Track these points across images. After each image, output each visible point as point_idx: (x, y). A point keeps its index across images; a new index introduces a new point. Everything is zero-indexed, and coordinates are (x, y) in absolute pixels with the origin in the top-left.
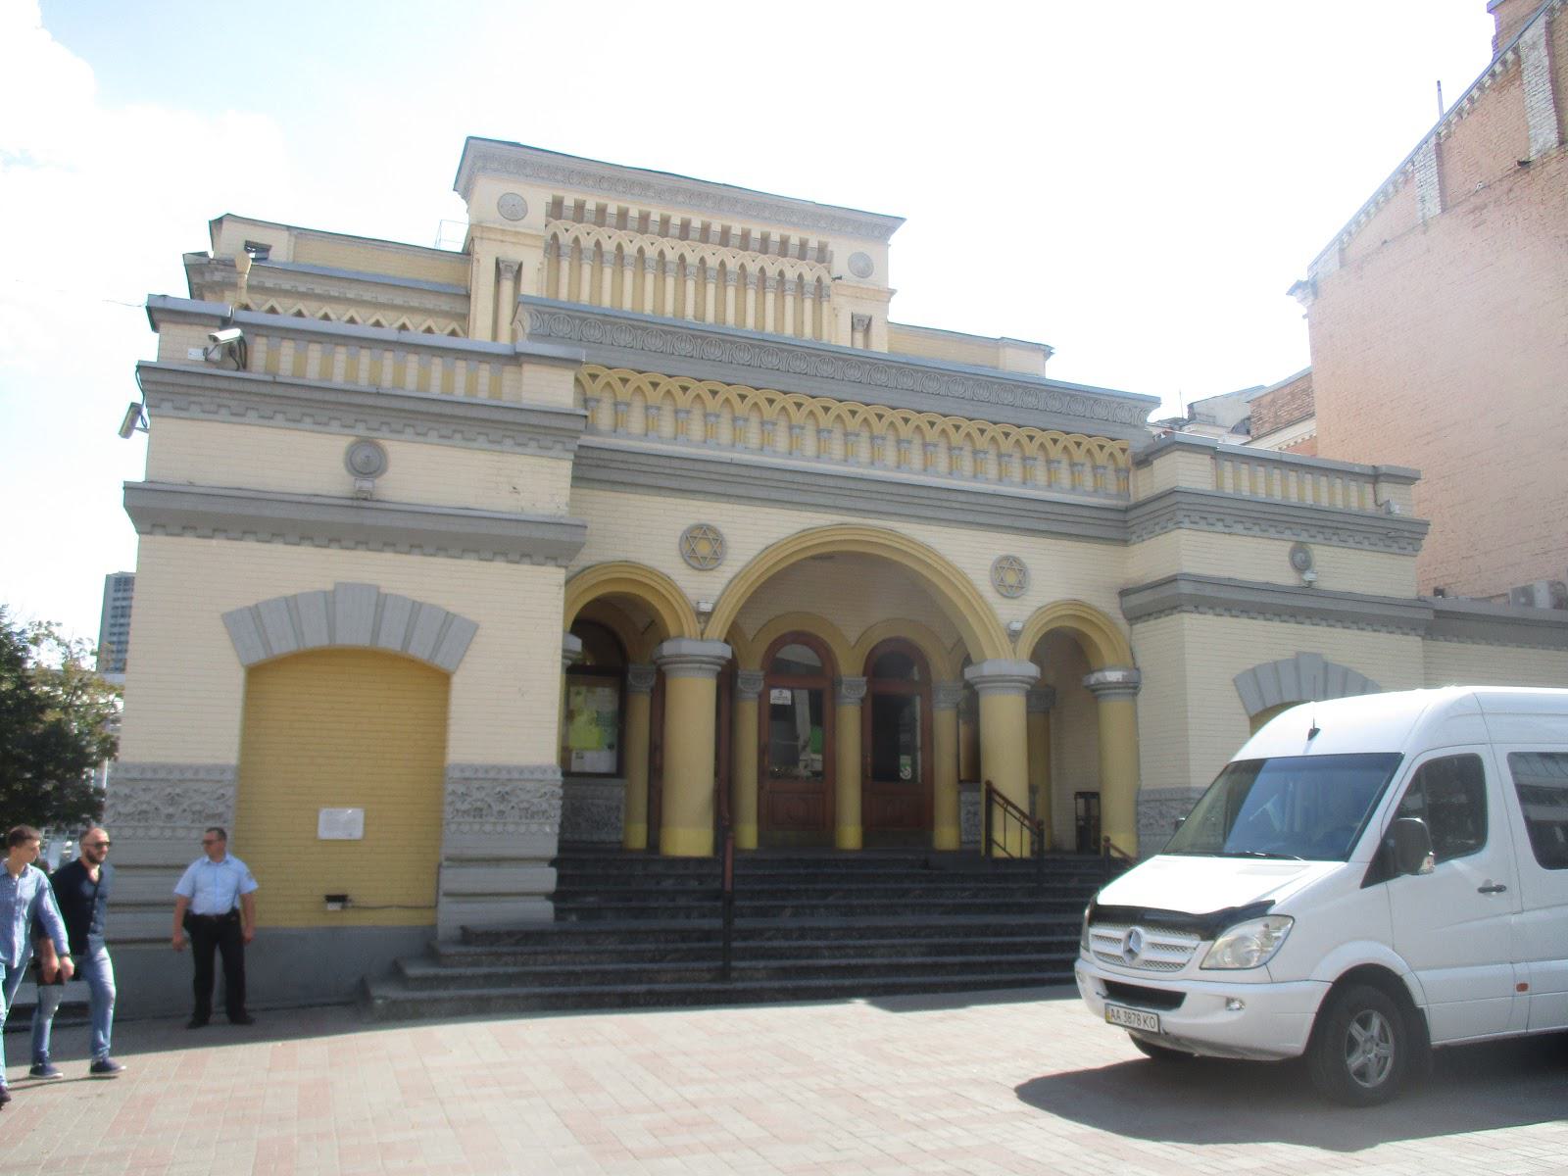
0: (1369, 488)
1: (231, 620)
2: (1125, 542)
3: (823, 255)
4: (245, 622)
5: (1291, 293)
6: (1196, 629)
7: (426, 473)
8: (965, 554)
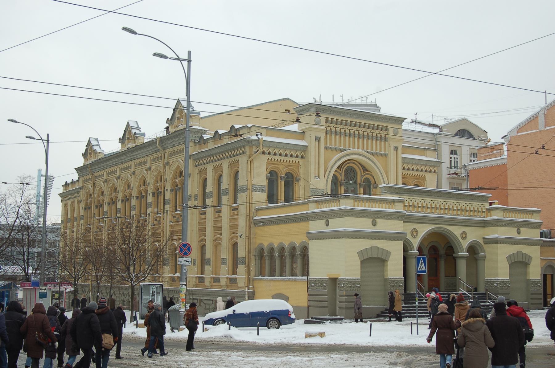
3: (387, 129)
4: (360, 253)
5: (502, 138)
7: (384, 226)
8: (456, 231)
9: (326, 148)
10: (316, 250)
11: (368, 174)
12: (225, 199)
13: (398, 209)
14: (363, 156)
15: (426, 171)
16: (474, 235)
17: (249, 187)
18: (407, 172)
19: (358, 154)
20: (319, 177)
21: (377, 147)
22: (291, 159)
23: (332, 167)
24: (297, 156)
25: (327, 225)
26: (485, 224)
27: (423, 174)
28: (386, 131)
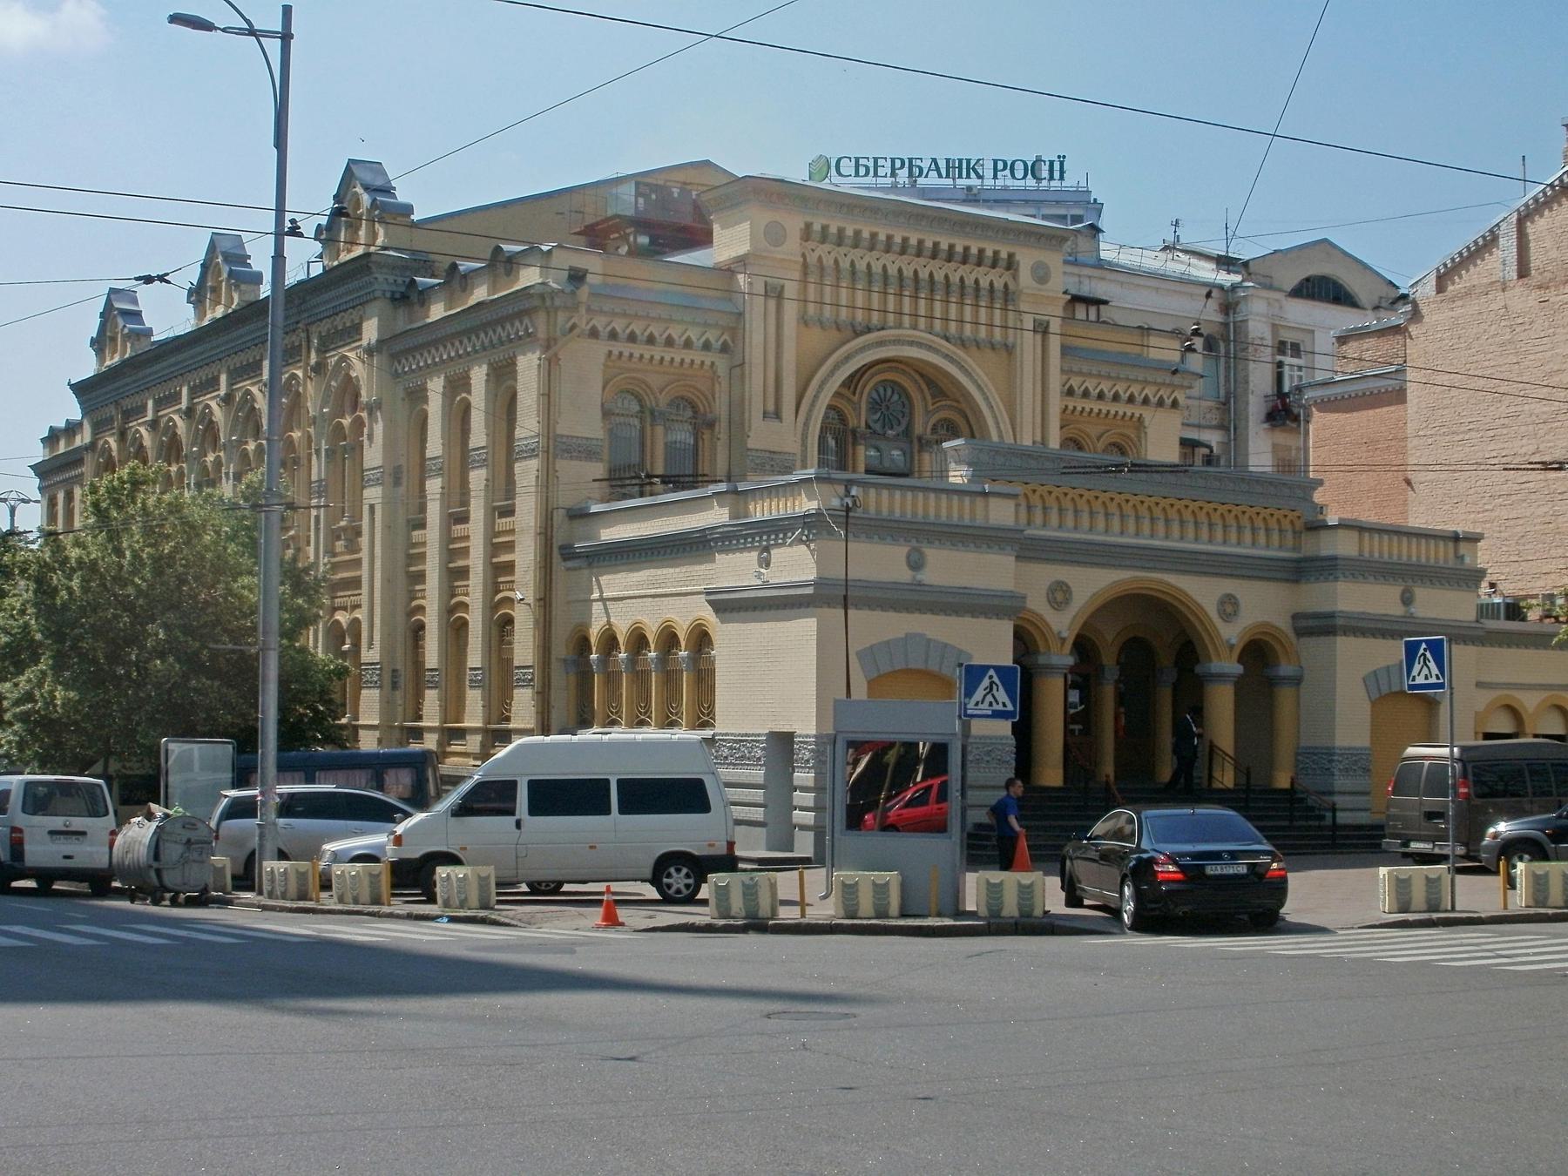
0: (1451, 545)
2: (1297, 581)
3: (1011, 264)
6: (1345, 646)
7: (948, 568)
8: (1202, 592)
9: (804, 321)
10: (733, 644)
11: (950, 407)
12: (478, 478)
13: (1002, 513)
14: (930, 348)
15: (1146, 401)
16: (1263, 606)
18: (1080, 404)
19: (911, 343)
20: (777, 415)
21: (980, 320)
22: (688, 356)
23: (823, 383)
24: (707, 346)
25: (767, 563)
26: (1301, 570)
27: (1137, 411)
28: (1009, 268)
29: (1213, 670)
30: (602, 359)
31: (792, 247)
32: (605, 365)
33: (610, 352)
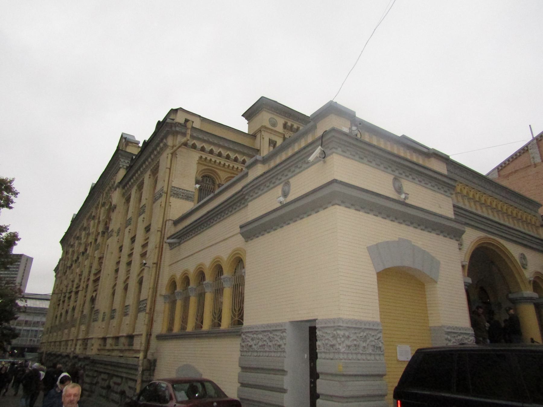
1: (369, 249)
4: (375, 251)
17: (165, 189)
29: (525, 296)
30: (197, 158)
31: (280, 128)
32: (198, 163)
33: (201, 157)
